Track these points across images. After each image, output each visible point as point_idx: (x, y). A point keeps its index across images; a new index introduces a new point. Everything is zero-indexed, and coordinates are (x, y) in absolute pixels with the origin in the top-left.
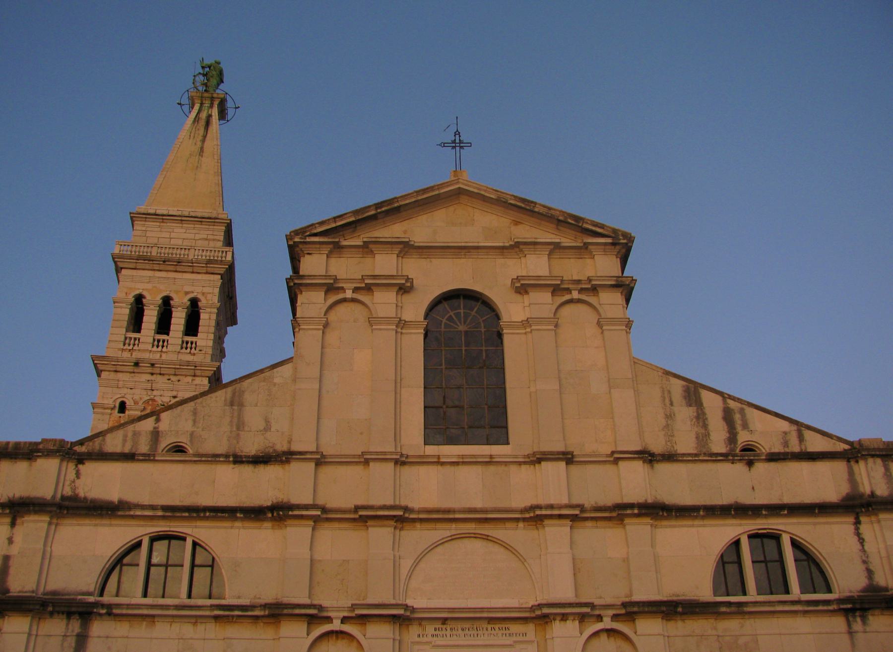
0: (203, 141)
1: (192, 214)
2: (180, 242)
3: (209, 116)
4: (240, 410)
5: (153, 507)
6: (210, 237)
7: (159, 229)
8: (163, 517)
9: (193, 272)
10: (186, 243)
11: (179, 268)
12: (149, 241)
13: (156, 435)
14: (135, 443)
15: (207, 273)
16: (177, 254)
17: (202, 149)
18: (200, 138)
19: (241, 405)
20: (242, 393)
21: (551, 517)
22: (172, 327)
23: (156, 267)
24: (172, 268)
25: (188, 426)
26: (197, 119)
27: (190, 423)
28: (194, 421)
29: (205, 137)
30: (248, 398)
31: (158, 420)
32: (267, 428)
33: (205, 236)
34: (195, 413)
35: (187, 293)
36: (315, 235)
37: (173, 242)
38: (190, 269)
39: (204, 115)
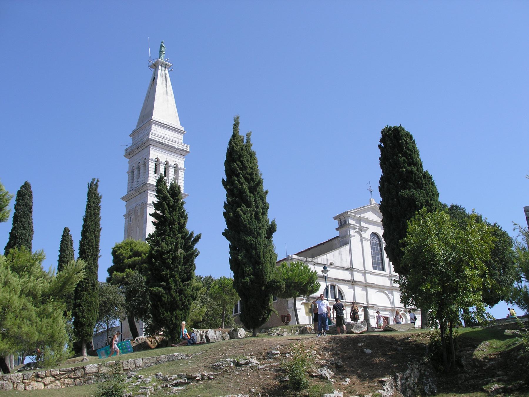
0: (167, 87)
1: (172, 125)
2: (168, 137)
3: (166, 74)
4: (341, 256)
5: (333, 278)
6: (179, 138)
7: (160, 129)
8: (333, 281)
9: (175, 153)
10: (171, 138)
11: (171, 150)
12: (158, 133)
13: (327, 259)
14: (324, 261)
15: (180, 154)
16: (172, 144)
17: (167, 91)
18: (165, 85)
19: (341, 255)
20: (341, 252)
21: (394, 289)
22: (170, 175)
23: (163, 147)
24: (169, 149)
25: (332, 258)
26: (161, 75)
27: (333, 258)
28: (334, 257)
29: (167, 85)
30: (342, 253)
31: (327, 256)
32: (347, 261)
33: (177, 137)
34: (333, 255)
35: (173, 161)
36: (351, 213)
37: (166, 136)
38: (175, 151)
39: (163, 72)
